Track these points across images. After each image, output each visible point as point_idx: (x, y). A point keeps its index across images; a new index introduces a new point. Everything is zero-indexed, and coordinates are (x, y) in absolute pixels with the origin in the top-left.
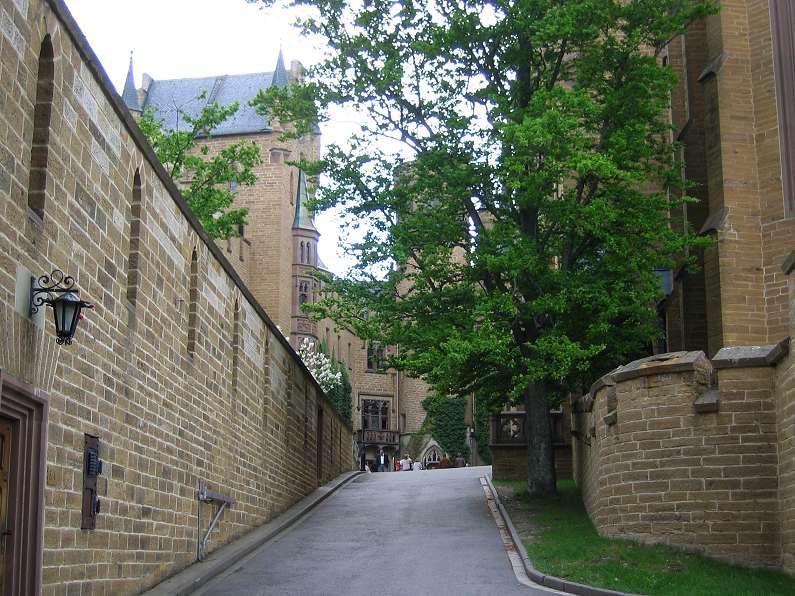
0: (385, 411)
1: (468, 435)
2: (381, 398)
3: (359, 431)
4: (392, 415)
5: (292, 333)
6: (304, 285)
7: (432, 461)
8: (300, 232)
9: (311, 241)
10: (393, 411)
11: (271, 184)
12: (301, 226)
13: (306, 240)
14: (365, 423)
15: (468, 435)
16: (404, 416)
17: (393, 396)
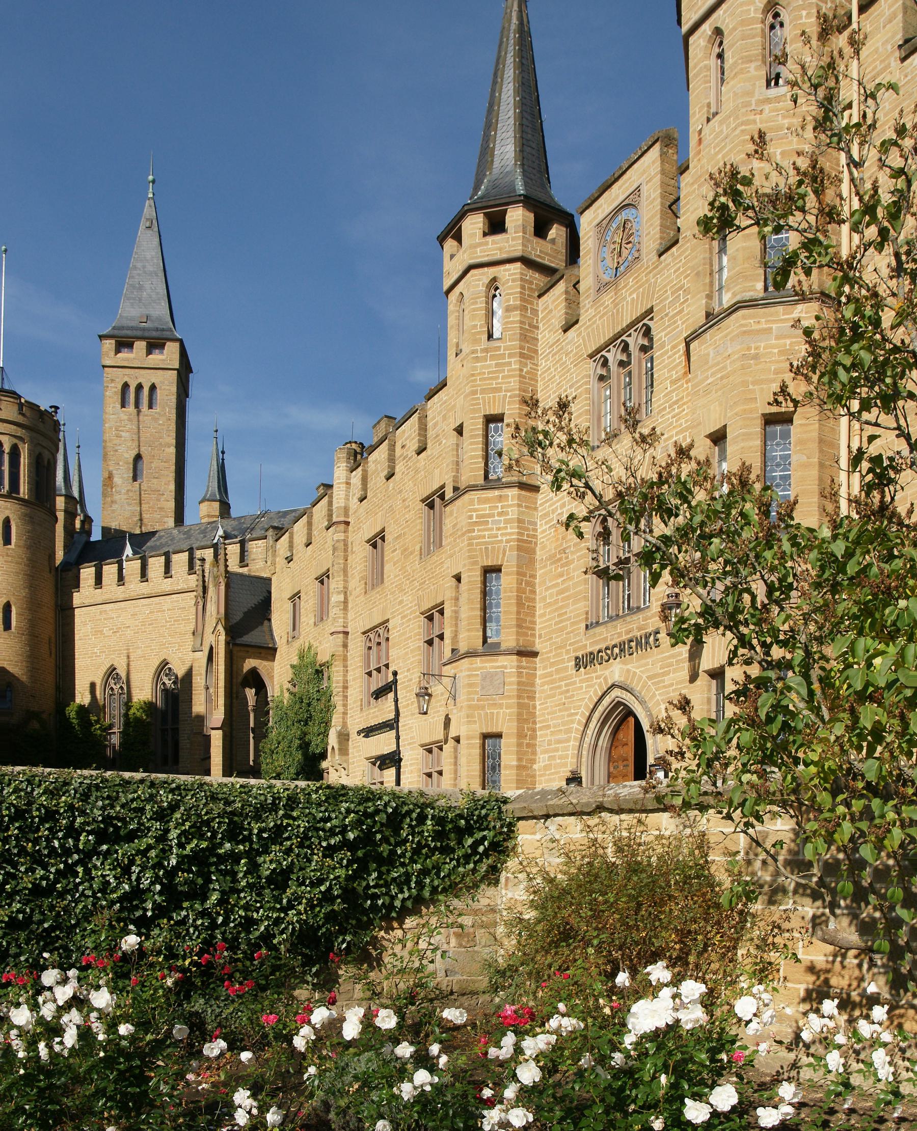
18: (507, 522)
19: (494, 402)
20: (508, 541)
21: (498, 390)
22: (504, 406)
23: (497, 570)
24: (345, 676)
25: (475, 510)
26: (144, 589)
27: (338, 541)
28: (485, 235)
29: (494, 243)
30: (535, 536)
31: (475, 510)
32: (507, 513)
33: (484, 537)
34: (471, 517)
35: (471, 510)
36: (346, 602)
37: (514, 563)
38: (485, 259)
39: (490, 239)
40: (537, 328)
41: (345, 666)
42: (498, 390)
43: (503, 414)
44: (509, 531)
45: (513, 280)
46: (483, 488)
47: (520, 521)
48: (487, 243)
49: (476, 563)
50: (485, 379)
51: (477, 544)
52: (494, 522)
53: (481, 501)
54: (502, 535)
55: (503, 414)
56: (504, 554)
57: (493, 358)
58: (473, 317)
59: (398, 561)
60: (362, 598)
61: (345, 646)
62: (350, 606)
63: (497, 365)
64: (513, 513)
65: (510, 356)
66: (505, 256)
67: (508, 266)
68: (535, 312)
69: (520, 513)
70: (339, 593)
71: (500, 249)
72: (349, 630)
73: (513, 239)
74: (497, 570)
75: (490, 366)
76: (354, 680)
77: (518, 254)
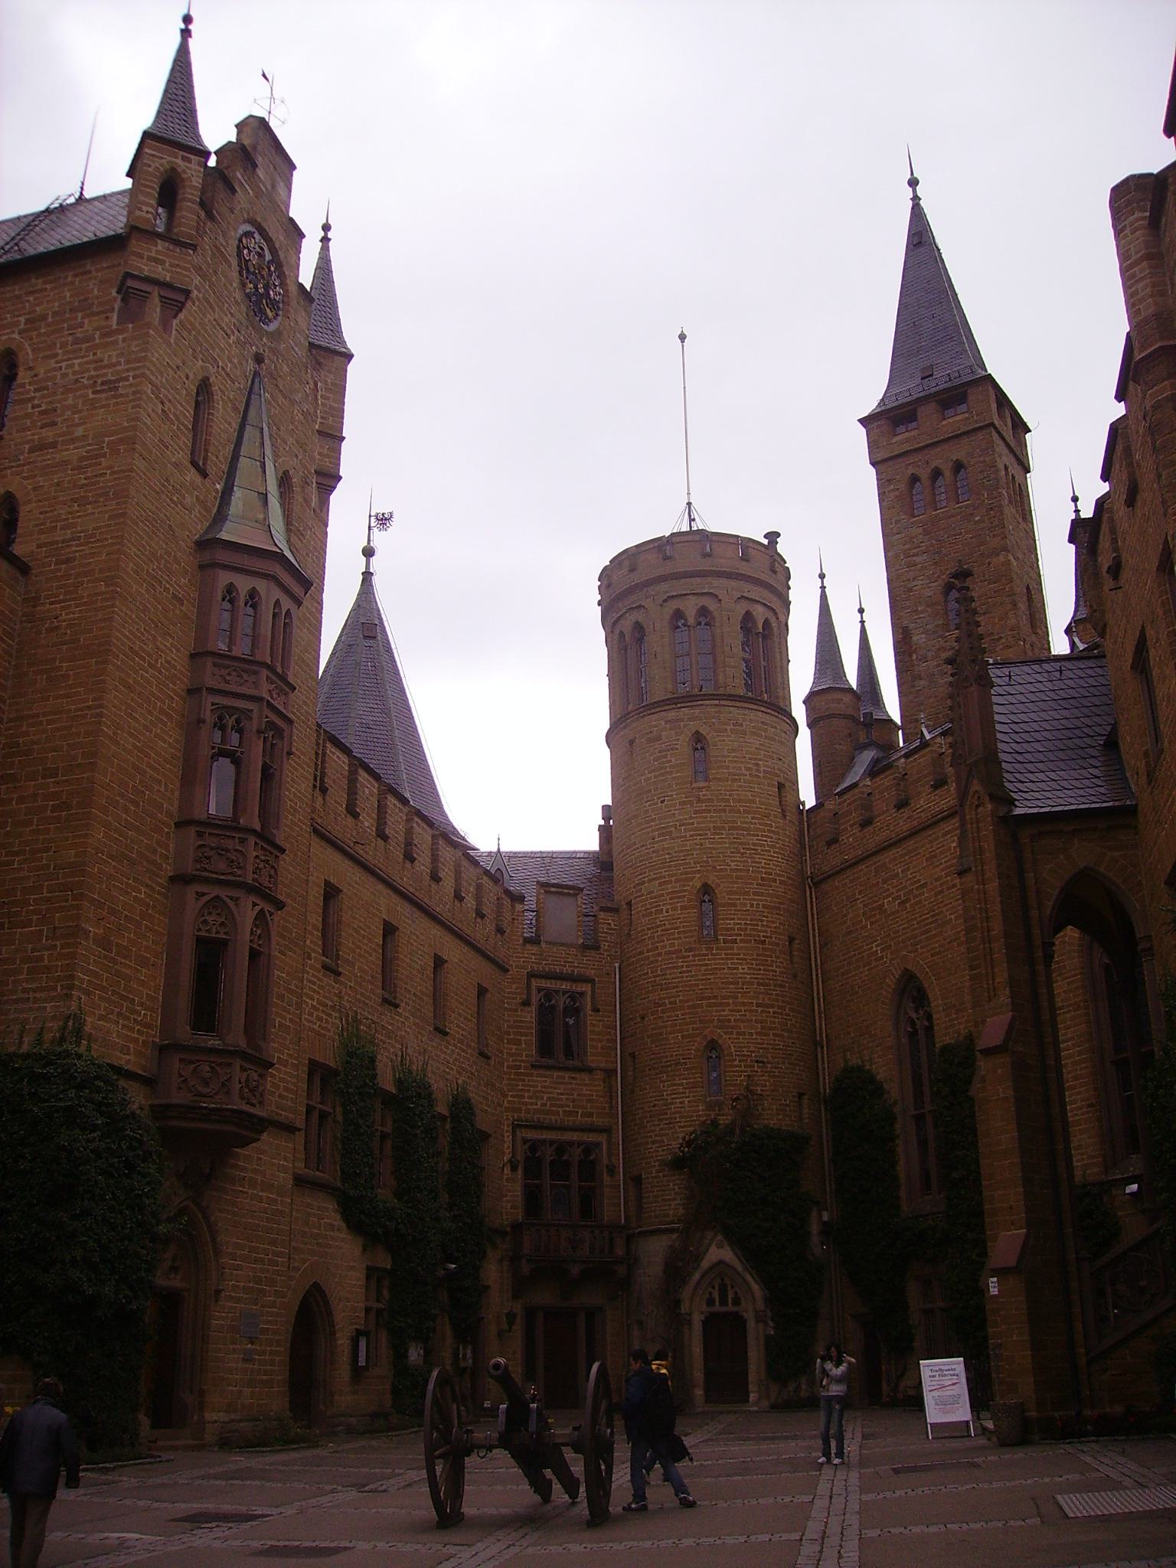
0: (589, 1168)
1: (815, 1228)
2: (575, 1136)
3: (517, 1227)
4: (606, 1178)
5: (173, 879)
6: (230, 722)
7: (718, 1308)
8: (223, 556)
9: (261, 586)
10: (612, 1170)
11: (111, 386)
12: (224, 535)
13: (244, 584)
14: (532, 1200)
15: (815, 1228)
16: (638, 1180)
17: (607, 1130)
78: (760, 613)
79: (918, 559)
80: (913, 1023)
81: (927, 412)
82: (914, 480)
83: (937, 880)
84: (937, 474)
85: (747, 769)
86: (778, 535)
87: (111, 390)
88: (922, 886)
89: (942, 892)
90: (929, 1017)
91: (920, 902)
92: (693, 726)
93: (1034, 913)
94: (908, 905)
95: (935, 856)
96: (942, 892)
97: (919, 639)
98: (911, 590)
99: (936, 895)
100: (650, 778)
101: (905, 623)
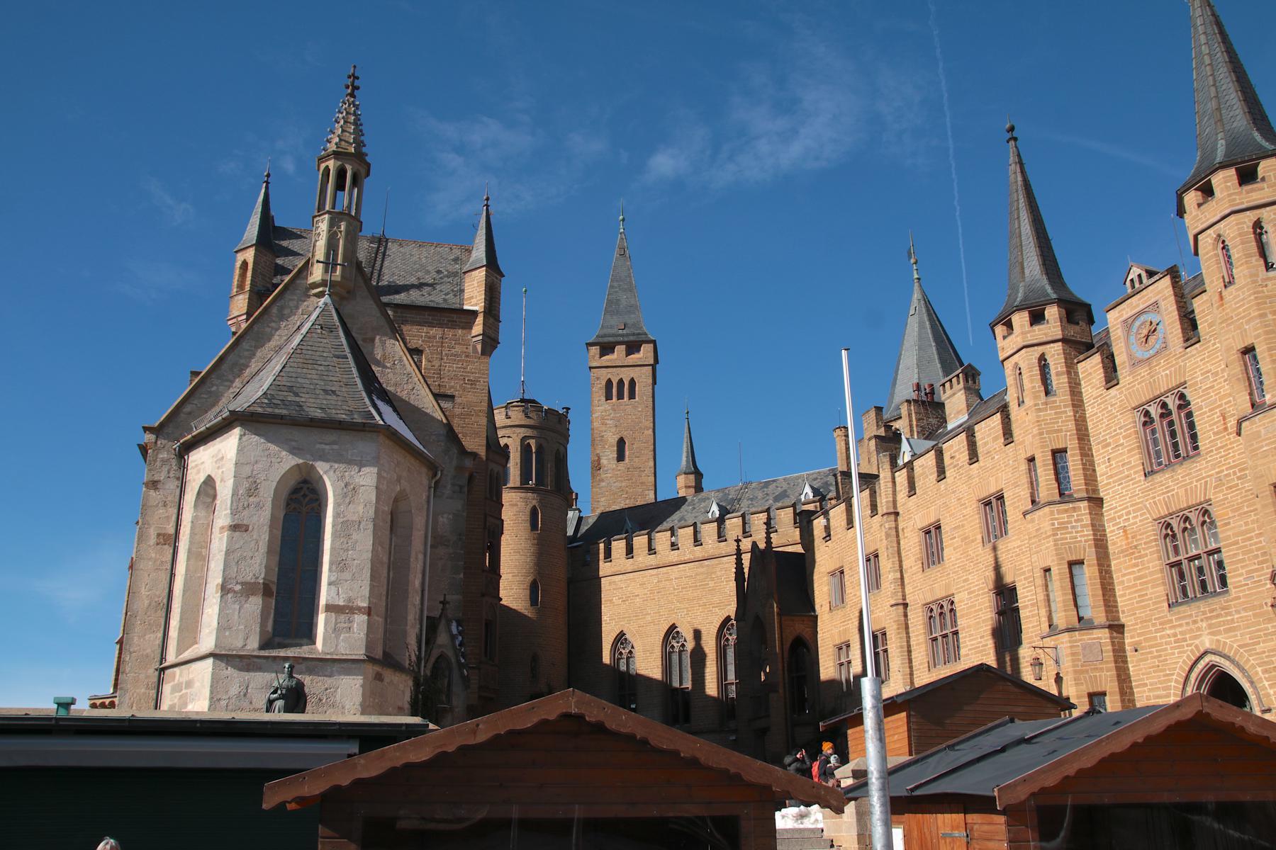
18: (1082, 526)
19: (1058, 439)
20: (1086, 541)
21: (1060, 431)
22: (1066, 442)
23: (1081, 562)
24: (908, 642)
25: (1056, 519)
26: (652, 560)
27: (890, 528)
28: (1031, 325)
29: (1039, 330)
30: (1105, 535)
31: (1056, 519)
32: (1082, 520)
33: (1066, 538)
34: (1053, 524)
35: (1052, 519)
36: (902, 578)
37: (1094, 557)
38: (1035, 342)
39: (1036, 328)
40: (1080, 384)
41: (908, 633)
42: (1060, 431)
43: (1066, 448)
44: (1086, 533)
45: (1058, 355)
46: (1060, 503)
47: (1093, 525)
48: (1034, 331)
49: (1063, 559)
50: (1048, 424)
51: (1062, 544)
52: (1073, 527)
53: (1059, 512)
54: (1081, 536)
55: (1066, 448)
56: (1085, 551)
57: (1051, 408)
58: (1032, 381)
59: (958, 547)
60: (920, 575)
61: (906, 615)
62: (906, 581)
63: (1056, 413)
64: (1087, 520)
65: (1065, 406)
66: (1050, 339)
67: (1052, 345)
68: (1077, 373)
69: (1092, 519)
70: (896, 571)
71: (1045, 334)
72: (908, 601)
73: (1054, 327)
74: (1081, 562)
75: (1050, 414)
76: (917, 645)
77: (1060, 337)
78: (562, 449)
79: (608, 422)
80: (621, 653)
81: (621, 349)
82: (609, 382)
83: (644, 595)
84: (621, 382)
85: (555, 526)
86: (569, 409)
87: (472, 384)
88: (636, 596)
89: (646, 600)
90: (630, 652)
91: (633, 603)
92: (534, 502)
93: (784, 647)
94: (627, 602)
95: (645, 584)
96: (646, 600)
97: (604, 461)
98: (603, 436)
99: (644, 601)
100: (510, 524)
101: (598, 452)
